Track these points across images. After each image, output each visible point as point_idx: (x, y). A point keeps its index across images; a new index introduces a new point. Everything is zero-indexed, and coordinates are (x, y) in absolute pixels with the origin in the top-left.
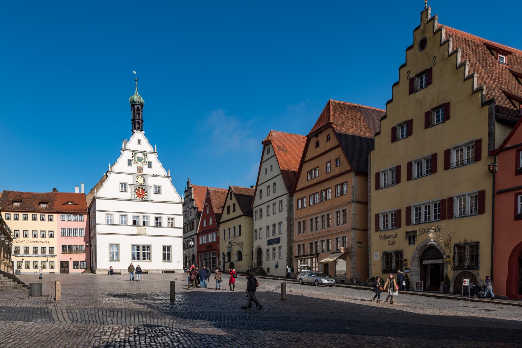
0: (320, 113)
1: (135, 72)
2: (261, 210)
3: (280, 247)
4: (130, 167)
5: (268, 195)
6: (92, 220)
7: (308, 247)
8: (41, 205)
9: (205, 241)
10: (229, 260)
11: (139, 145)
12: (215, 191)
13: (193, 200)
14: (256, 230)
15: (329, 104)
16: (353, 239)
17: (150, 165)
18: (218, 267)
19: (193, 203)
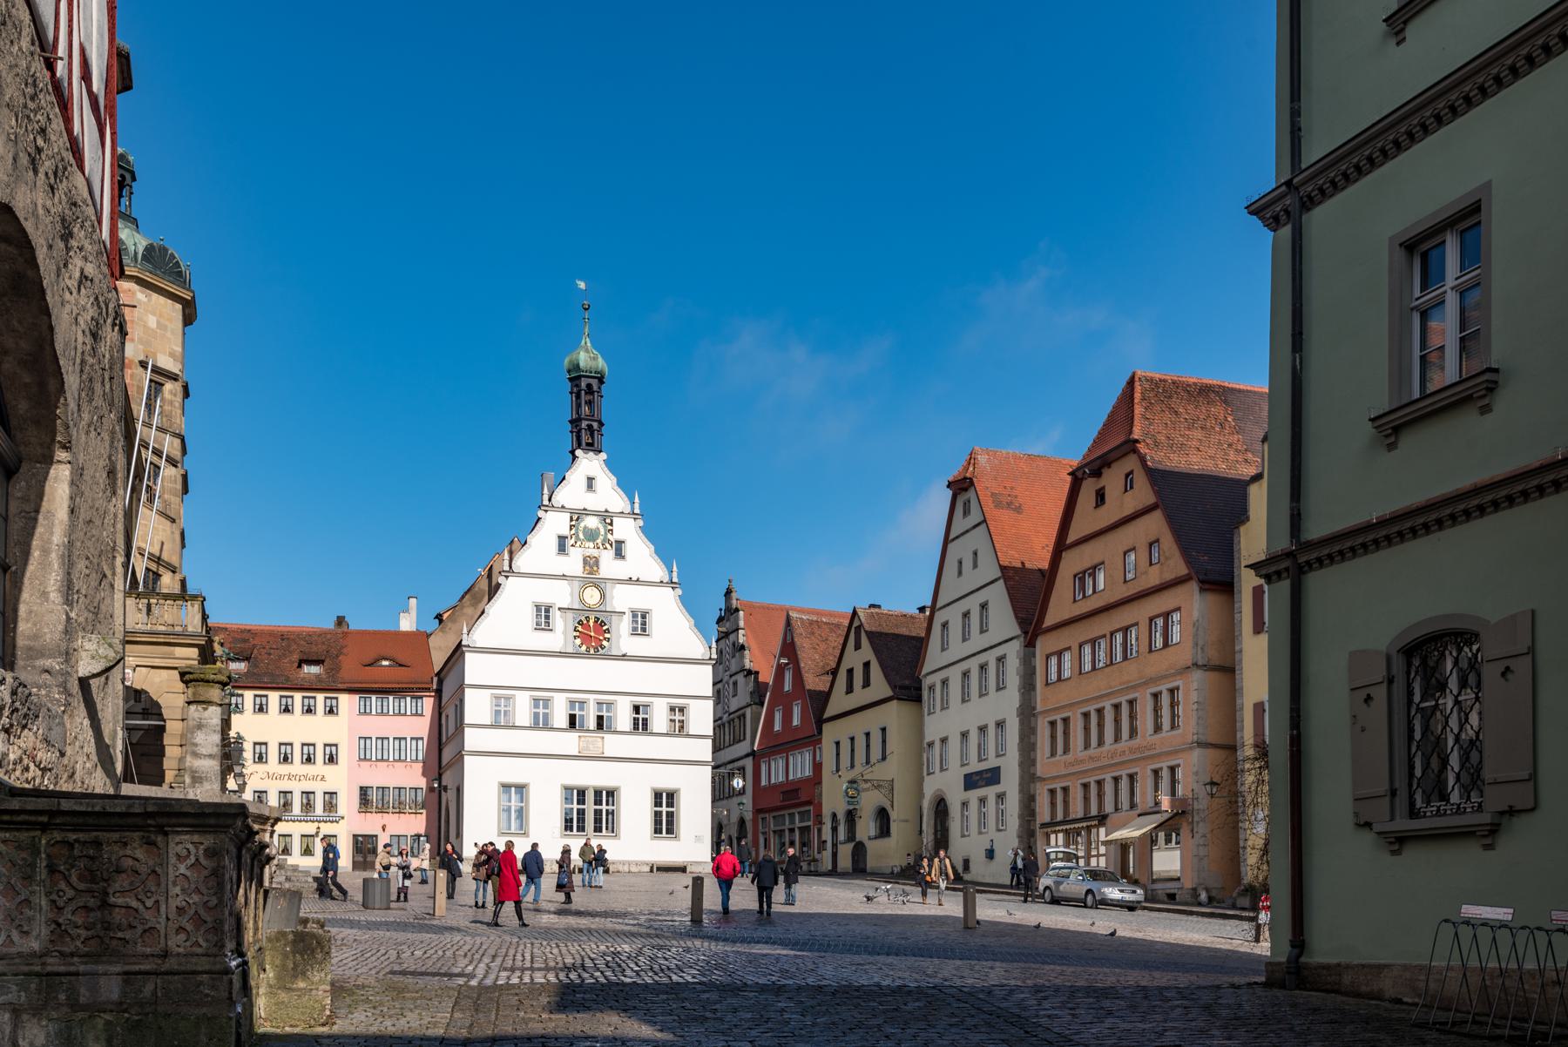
0: (1109, 409)
1: (582, 285)
2: (945, 682)
3: (1001, 797)
4: (562, 558)
5: (964, 640)
6: (450, 711)
7: (1077, 795)
8: (306, 669)
9: (778, 777)
10: (851, 836)
11: (590, 495)
12: (811, 623)
13: (742, 648)
14: (931, 745)
15: (1131, 382)
16: (1197, 773)
17: (619, 550)
18: (817, 856)
19: (743, 657)
